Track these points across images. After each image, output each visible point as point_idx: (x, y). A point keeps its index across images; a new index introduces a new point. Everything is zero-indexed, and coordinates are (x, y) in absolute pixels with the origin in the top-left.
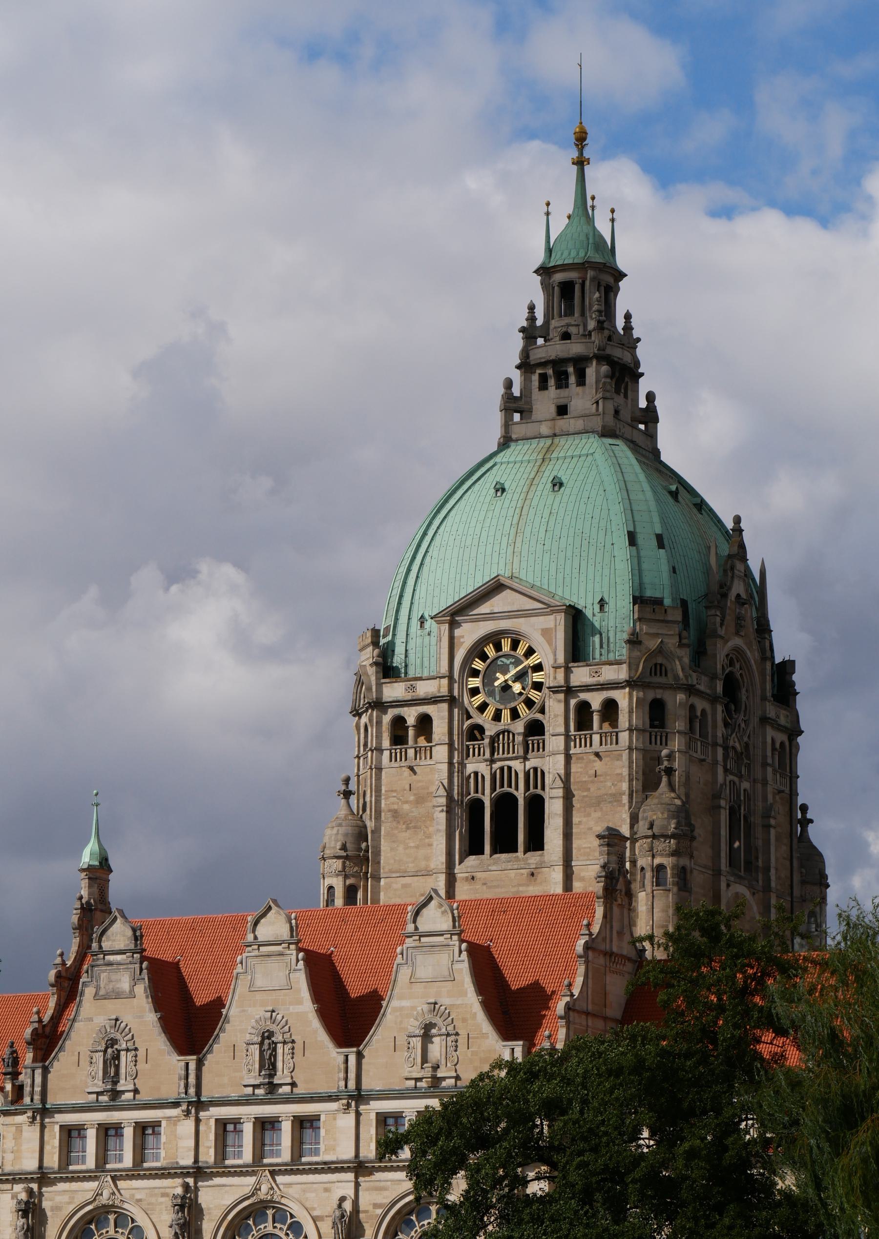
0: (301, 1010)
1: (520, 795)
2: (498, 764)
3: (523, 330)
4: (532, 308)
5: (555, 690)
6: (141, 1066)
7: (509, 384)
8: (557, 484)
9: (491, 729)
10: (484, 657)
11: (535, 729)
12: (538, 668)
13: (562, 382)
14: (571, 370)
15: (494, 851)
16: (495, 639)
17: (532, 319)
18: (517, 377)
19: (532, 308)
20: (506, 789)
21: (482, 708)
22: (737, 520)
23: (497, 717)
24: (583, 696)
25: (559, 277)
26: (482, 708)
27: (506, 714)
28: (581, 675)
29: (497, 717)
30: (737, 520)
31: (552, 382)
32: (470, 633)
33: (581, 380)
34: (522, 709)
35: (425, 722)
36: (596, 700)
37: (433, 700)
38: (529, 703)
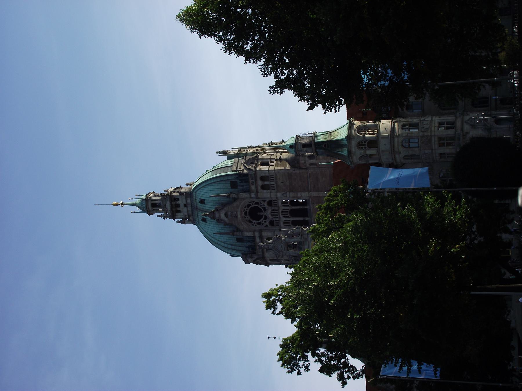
1: (289, 208)
2: (281, 216)
3: (164, 219)
4: (158, 216)
7: (178, 222)
11: (270, 203)
14: (173, 203)
17: (161, 216)
18: (176, 220)
19: (158, 216)
20: (288, 213)
22: (217, 153)
24: (259, 188)
25: (150, 208)
28: (253, 188)
30: (217, 153)
31: (178, 209)
33: (178, 200)
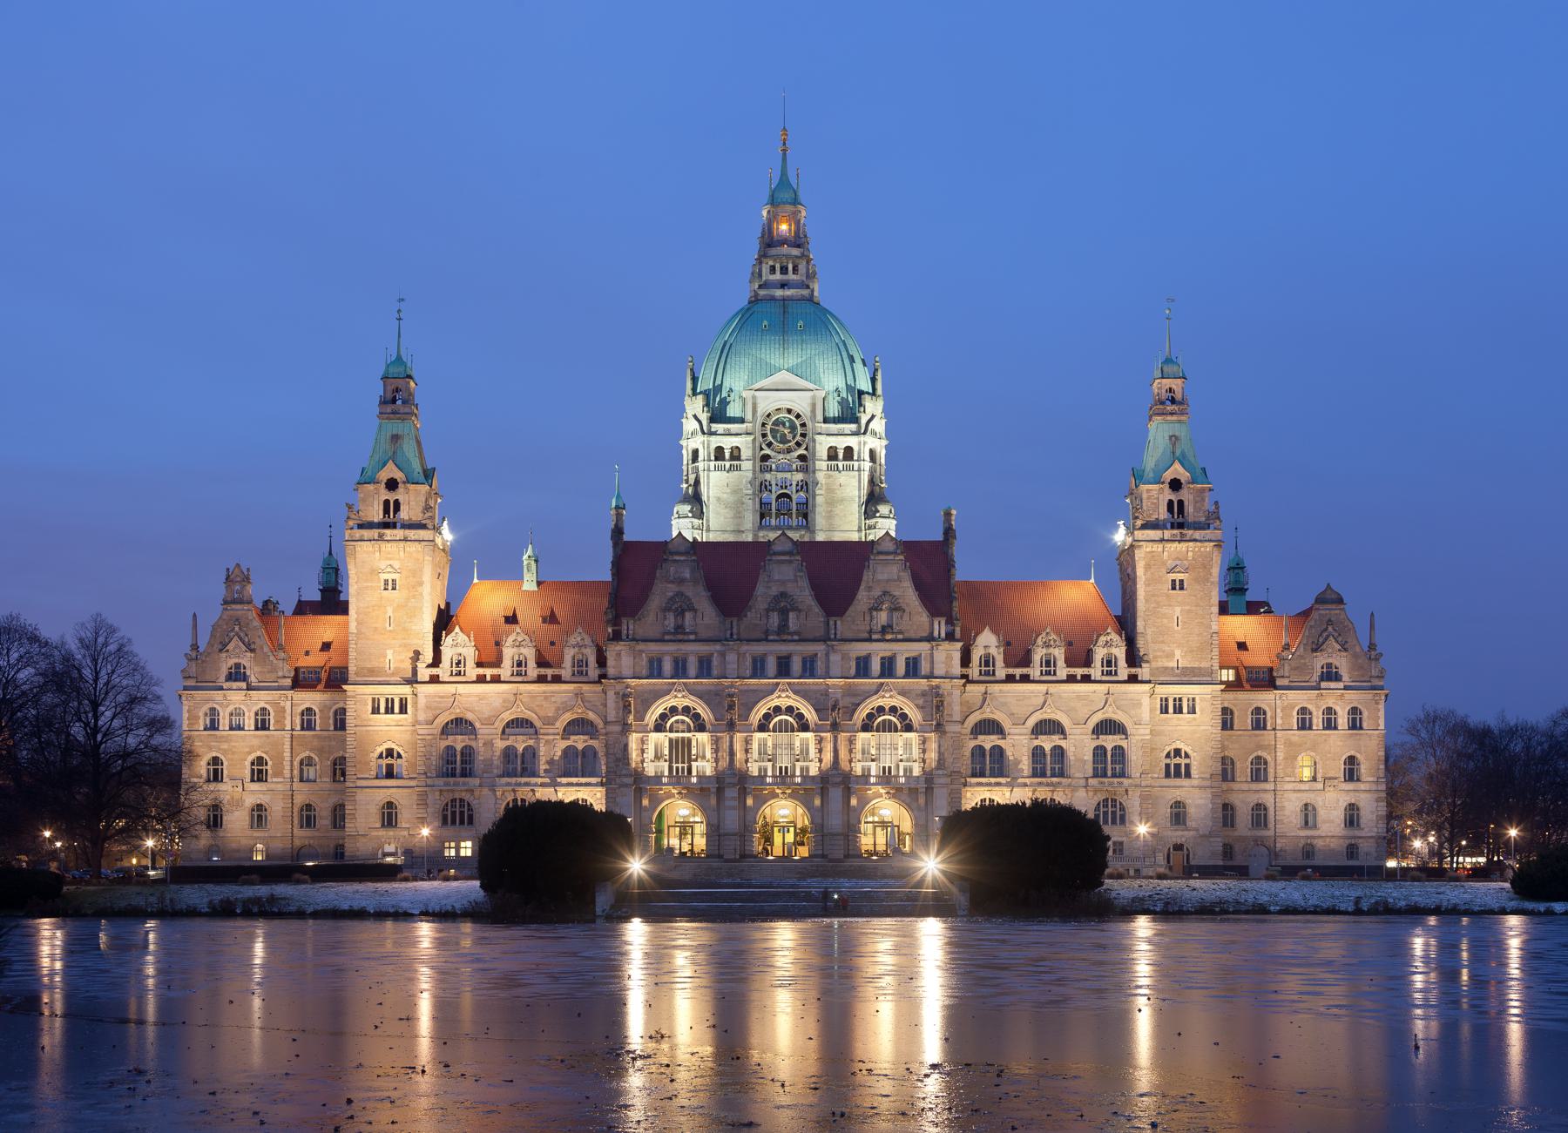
0: (804, 594)
6: (699, 621)
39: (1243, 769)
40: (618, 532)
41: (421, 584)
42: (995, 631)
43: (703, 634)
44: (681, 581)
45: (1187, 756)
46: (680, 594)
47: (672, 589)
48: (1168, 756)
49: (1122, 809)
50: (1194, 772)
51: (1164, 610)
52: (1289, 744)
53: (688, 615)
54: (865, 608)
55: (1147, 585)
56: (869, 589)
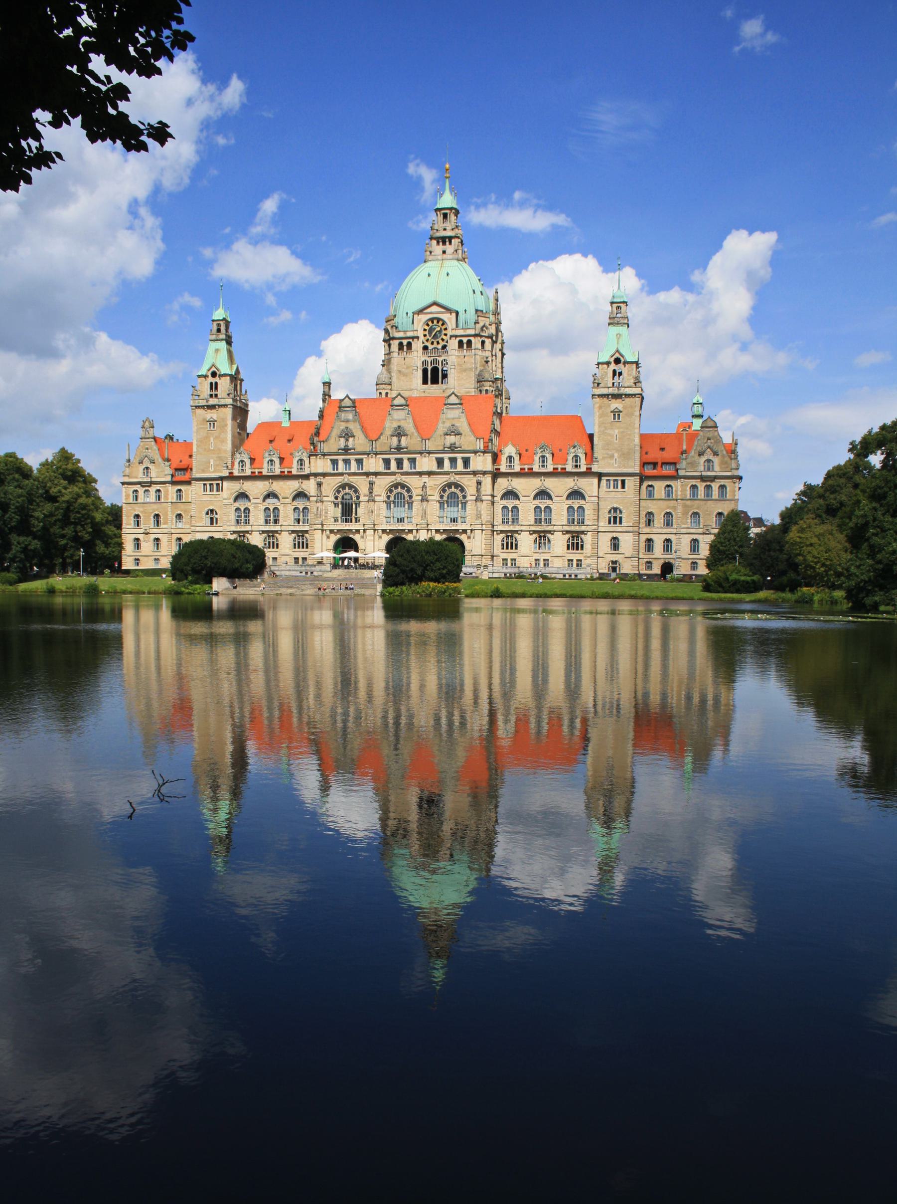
0: (409, 426)
5: (451, 336)
8: (448, 274)
9: (430, 347)
10: (428, 325)
11: (444, 347)
12: (446, 329)
13: (444, 243)
15: (432, 383)
16: (432, 320)
21: (427, 340)
23: (432, 343)
26: (427, 340)
27: (435, 343)
29: (432, 343)
32: (424, 318)
33: (450, 243)
34: (440, 341)
35: (409, 345)
36: (465, 340)
37: (413, 338)
38: (443, 340)
39: (659, 520)
40: (326, 396)
41: (226, 425)
42: (514, 446)
43: (359, 449)
44: (348, 421)
45: (621, 512)
46: (347, 428)
47: (343, 426)
48: (610, 512)
49: (582, 541)
50: (623, 521)
51: (609, 431)
52: (685, 506)
53: (351, 439)
54: (442, 433)
55: (601, 416)
56: (444, 422)
